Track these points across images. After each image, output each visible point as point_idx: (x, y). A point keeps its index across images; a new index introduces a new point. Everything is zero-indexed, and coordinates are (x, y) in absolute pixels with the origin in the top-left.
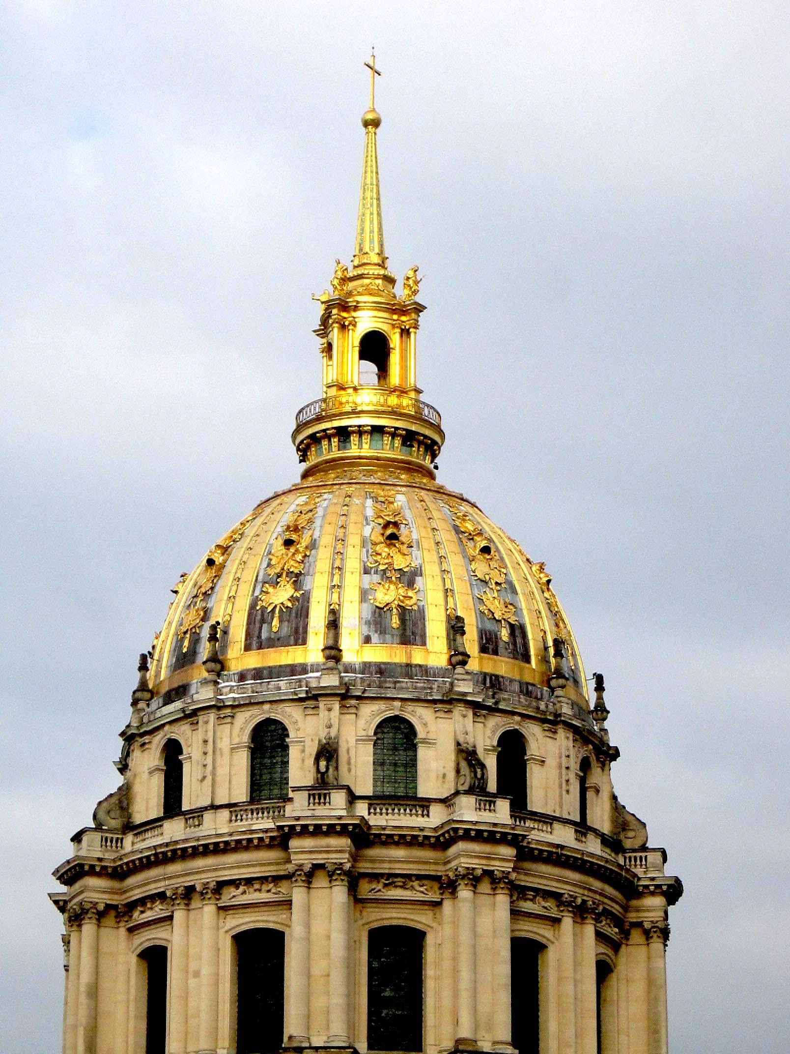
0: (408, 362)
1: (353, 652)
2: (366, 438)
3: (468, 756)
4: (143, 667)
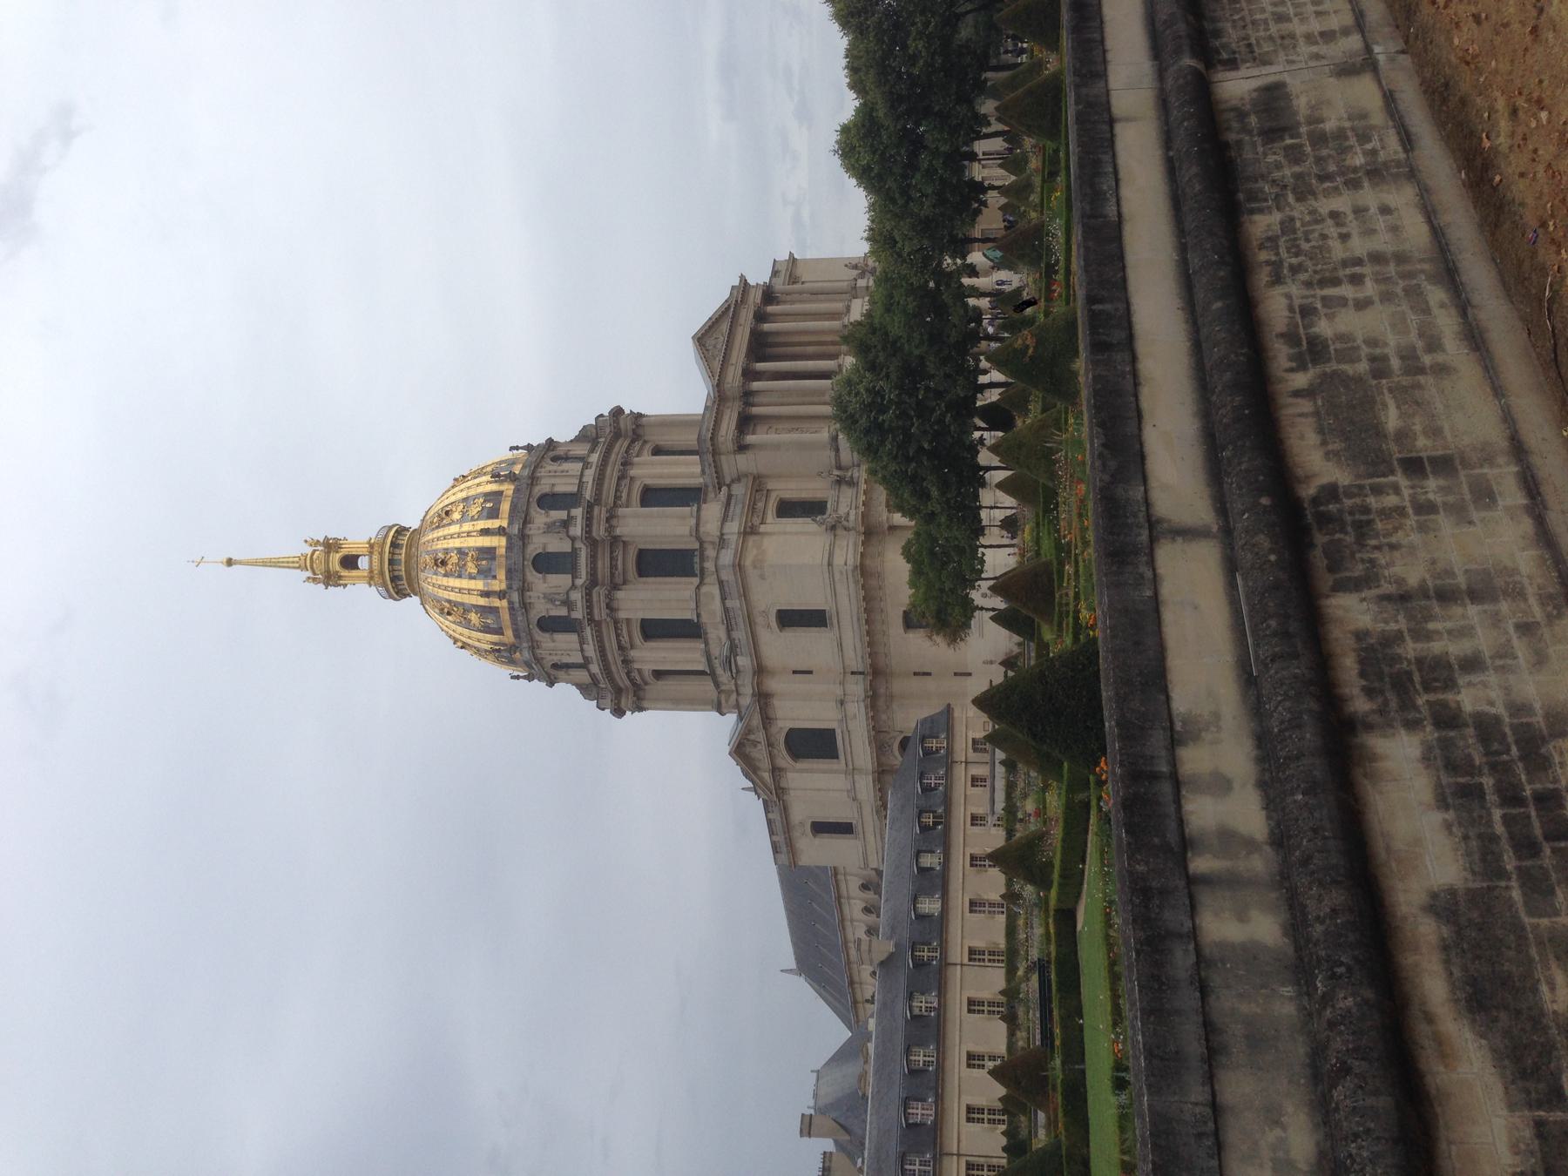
3: (550, 528)
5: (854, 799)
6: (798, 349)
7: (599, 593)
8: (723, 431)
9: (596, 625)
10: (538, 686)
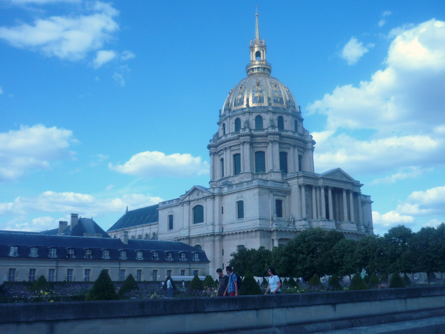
1: (251, 104)
2: (257, 70)
3: (271, 121)
4: (220, 112)
5: (180, 230)
6: (337, 205)
8: (306, 180)
10: (217, 119)
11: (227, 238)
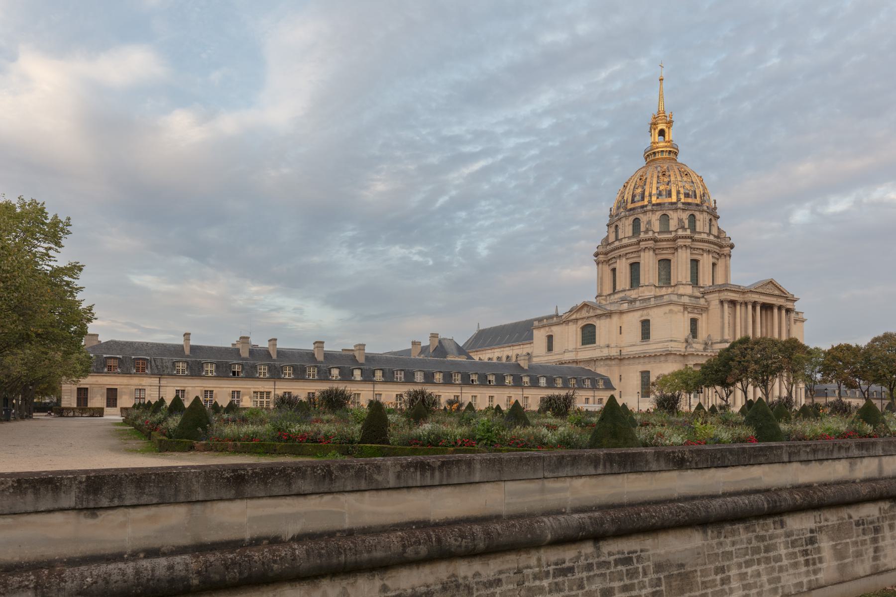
0: (671, 135)
3: (680, 220)
7: (651, 244)
8: (730, 294)
9: (638, 243)
11: (626, 362)
